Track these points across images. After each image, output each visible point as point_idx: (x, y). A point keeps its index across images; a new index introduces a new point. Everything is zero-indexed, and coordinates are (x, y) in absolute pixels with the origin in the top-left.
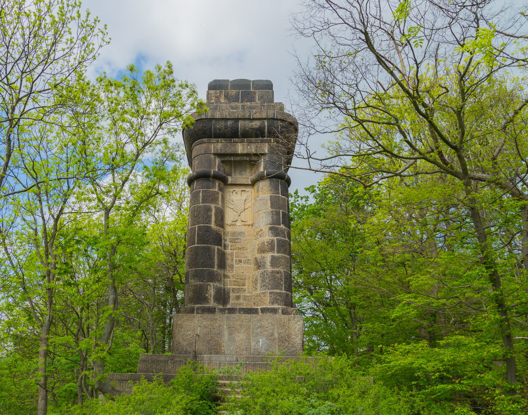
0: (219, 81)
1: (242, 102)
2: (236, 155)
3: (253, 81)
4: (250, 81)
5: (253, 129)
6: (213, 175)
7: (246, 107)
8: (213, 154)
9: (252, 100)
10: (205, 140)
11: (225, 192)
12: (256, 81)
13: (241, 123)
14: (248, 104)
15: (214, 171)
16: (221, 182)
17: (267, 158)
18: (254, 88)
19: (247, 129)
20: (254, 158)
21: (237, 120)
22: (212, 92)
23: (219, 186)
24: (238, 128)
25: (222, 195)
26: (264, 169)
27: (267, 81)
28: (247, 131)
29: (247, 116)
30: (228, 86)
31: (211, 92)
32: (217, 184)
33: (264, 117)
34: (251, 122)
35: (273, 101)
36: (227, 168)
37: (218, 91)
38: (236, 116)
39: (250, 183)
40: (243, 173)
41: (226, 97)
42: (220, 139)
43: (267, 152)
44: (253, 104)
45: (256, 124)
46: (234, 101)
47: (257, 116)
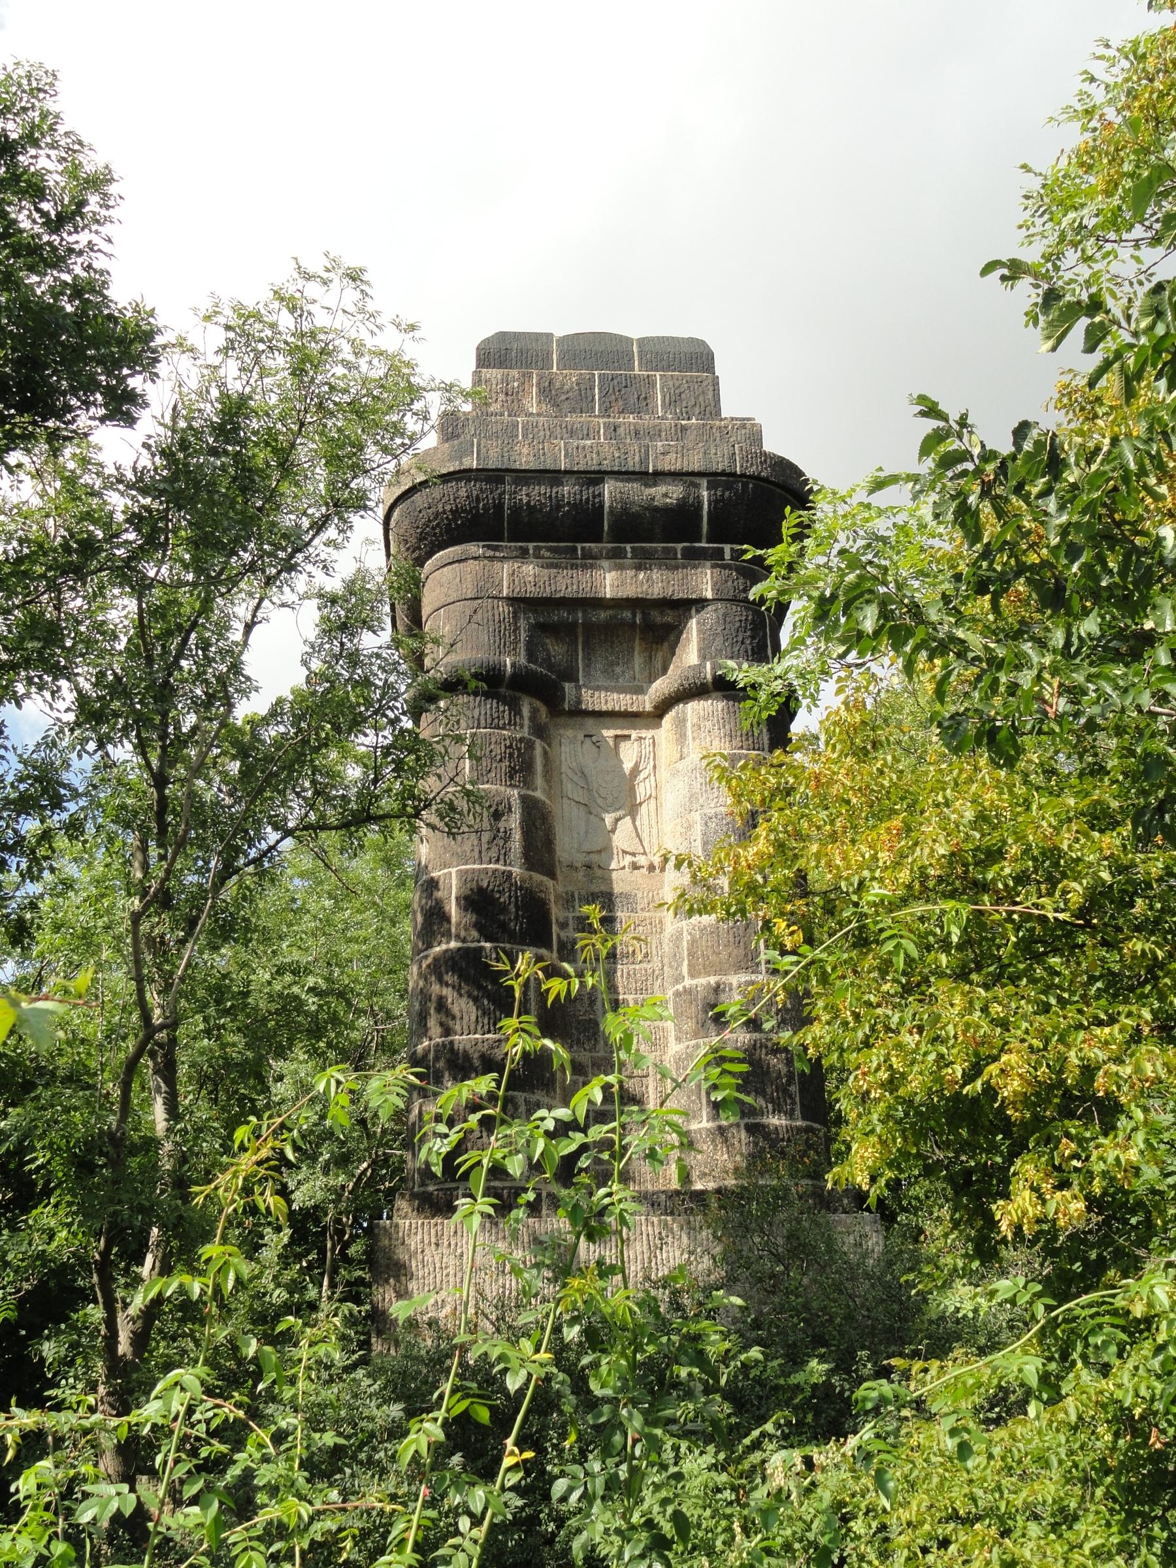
0: (517, 336)
1: (606, 411)
2: (597, 603)
3: (642, 342)
4: (629, 340)
5: (656, 509)
6: (514, 675)
7: (621, 430)
8: (508, 598)
9: (643, 404)
10: (475, 548)
11: (555, 743)
12: (653, 339)
13: (609, 490)
14: (631, 419)
15: (513, 665)
16: (538, 704)
17: (710, 615)
18: (646, 364)
19: (635, 509)
20: (658, 618)
21: (595, 477)
22: (494, 374)
23: (533, 717)
24: (602, 506)
25: (545, 753)
26: (703, 657)
27: (692, 340)
28: (636, 516)
29: (633, 464)
30: (549, 354)
31: (487, 373)
32: (526, 711)
33: (696, 467)
34: (647, 485)
35: (718, 412)
36: (556, 650)
37: (515, 373)
38: (590, 462)
39: (648, 707)
40: (618, 670)
41: (547, 392)
42: (531, 545)
43: (709, 595)
44: (647, 420)
45: (668, 494)
46: (573, 411)
47: (670, 463)
